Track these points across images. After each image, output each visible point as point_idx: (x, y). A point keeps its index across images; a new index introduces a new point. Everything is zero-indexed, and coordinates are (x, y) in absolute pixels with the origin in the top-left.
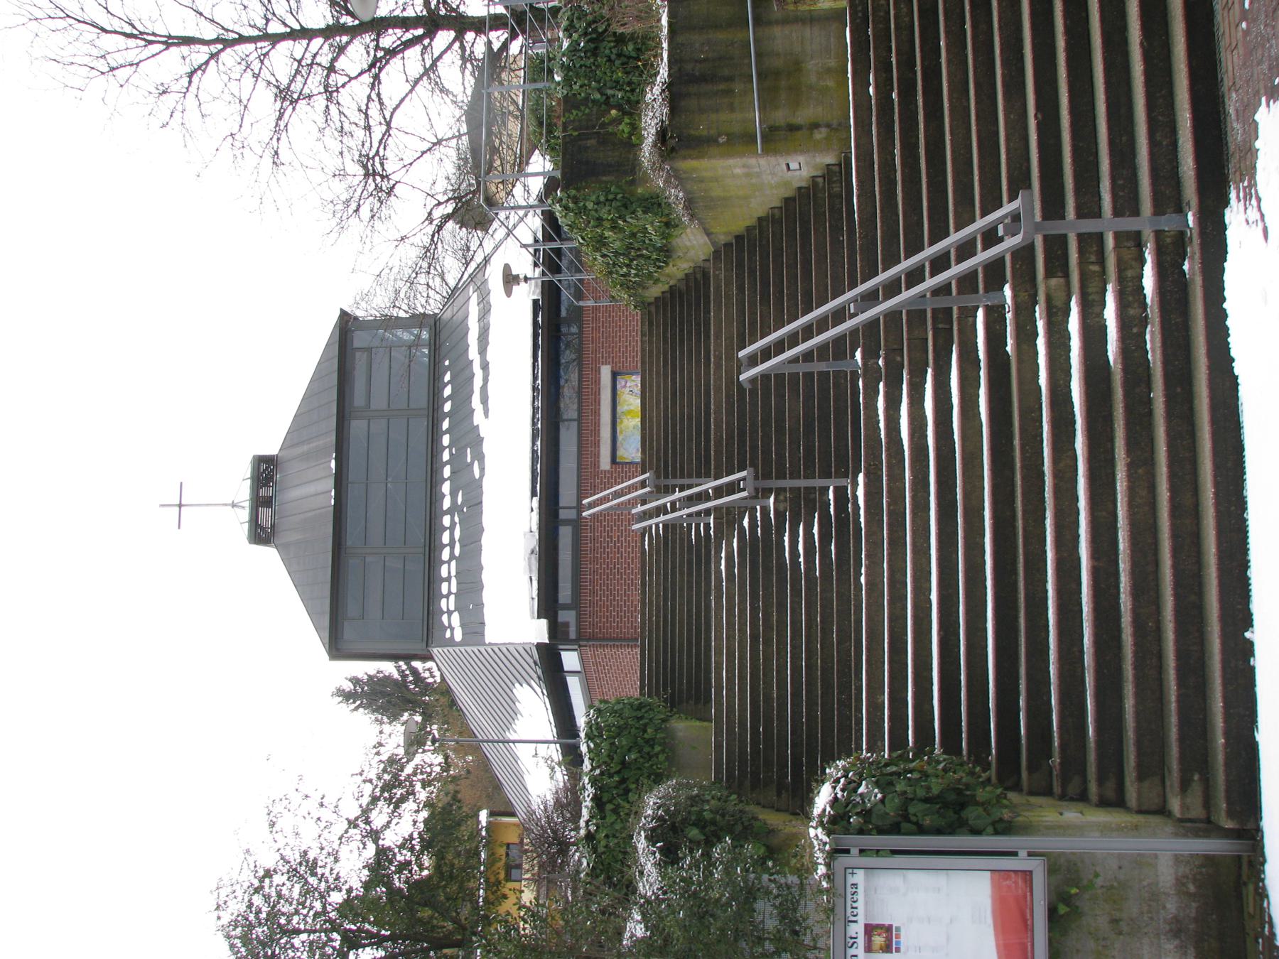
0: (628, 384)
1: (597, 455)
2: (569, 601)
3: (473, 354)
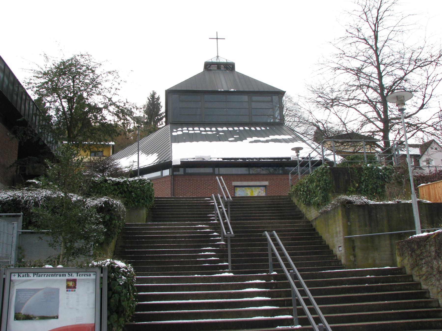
0: (262, 191)
1: (237, 181)
2: (187, 172)
3: (272, 137)
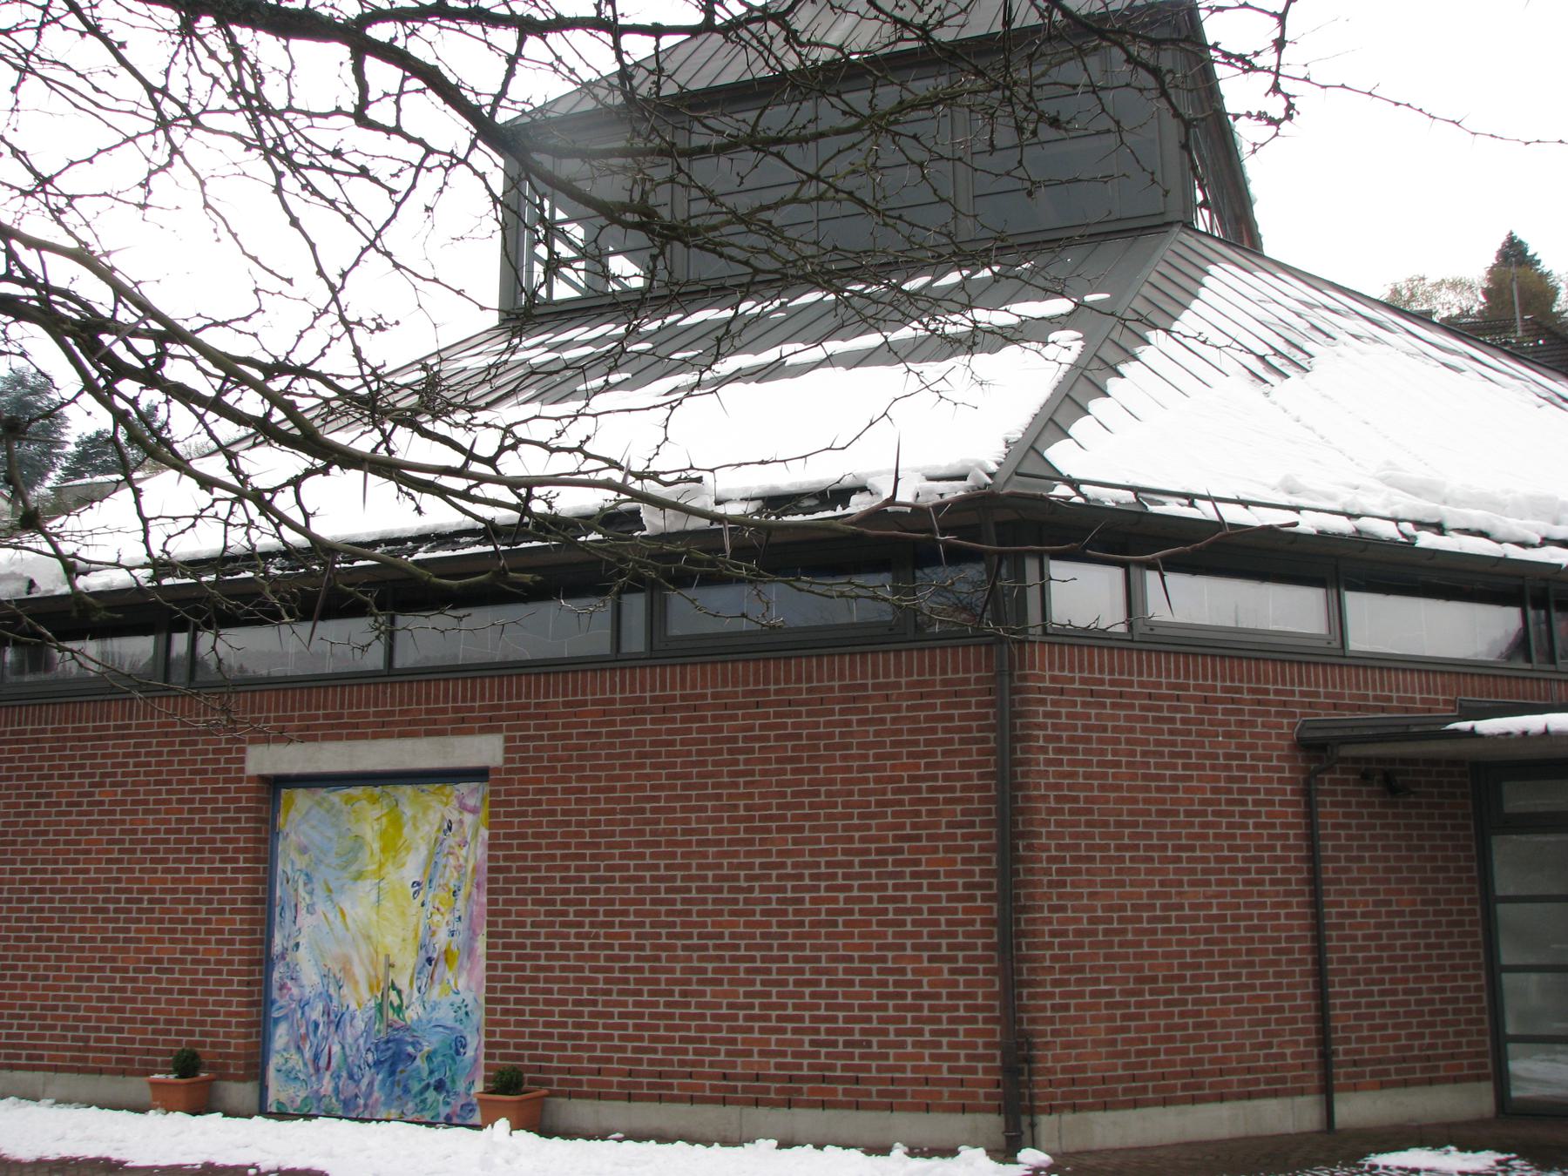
0: (468, 818)
1: (282, 737)
2: (676, 628)
3: (834, 346)
